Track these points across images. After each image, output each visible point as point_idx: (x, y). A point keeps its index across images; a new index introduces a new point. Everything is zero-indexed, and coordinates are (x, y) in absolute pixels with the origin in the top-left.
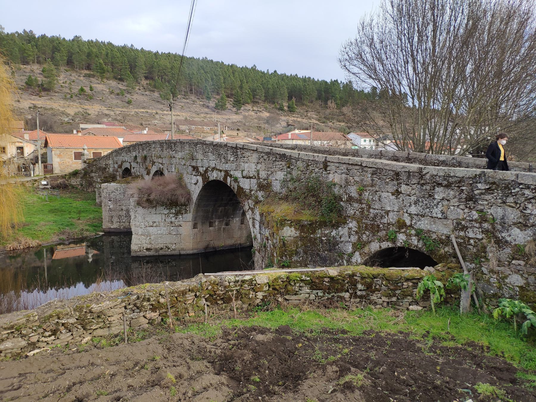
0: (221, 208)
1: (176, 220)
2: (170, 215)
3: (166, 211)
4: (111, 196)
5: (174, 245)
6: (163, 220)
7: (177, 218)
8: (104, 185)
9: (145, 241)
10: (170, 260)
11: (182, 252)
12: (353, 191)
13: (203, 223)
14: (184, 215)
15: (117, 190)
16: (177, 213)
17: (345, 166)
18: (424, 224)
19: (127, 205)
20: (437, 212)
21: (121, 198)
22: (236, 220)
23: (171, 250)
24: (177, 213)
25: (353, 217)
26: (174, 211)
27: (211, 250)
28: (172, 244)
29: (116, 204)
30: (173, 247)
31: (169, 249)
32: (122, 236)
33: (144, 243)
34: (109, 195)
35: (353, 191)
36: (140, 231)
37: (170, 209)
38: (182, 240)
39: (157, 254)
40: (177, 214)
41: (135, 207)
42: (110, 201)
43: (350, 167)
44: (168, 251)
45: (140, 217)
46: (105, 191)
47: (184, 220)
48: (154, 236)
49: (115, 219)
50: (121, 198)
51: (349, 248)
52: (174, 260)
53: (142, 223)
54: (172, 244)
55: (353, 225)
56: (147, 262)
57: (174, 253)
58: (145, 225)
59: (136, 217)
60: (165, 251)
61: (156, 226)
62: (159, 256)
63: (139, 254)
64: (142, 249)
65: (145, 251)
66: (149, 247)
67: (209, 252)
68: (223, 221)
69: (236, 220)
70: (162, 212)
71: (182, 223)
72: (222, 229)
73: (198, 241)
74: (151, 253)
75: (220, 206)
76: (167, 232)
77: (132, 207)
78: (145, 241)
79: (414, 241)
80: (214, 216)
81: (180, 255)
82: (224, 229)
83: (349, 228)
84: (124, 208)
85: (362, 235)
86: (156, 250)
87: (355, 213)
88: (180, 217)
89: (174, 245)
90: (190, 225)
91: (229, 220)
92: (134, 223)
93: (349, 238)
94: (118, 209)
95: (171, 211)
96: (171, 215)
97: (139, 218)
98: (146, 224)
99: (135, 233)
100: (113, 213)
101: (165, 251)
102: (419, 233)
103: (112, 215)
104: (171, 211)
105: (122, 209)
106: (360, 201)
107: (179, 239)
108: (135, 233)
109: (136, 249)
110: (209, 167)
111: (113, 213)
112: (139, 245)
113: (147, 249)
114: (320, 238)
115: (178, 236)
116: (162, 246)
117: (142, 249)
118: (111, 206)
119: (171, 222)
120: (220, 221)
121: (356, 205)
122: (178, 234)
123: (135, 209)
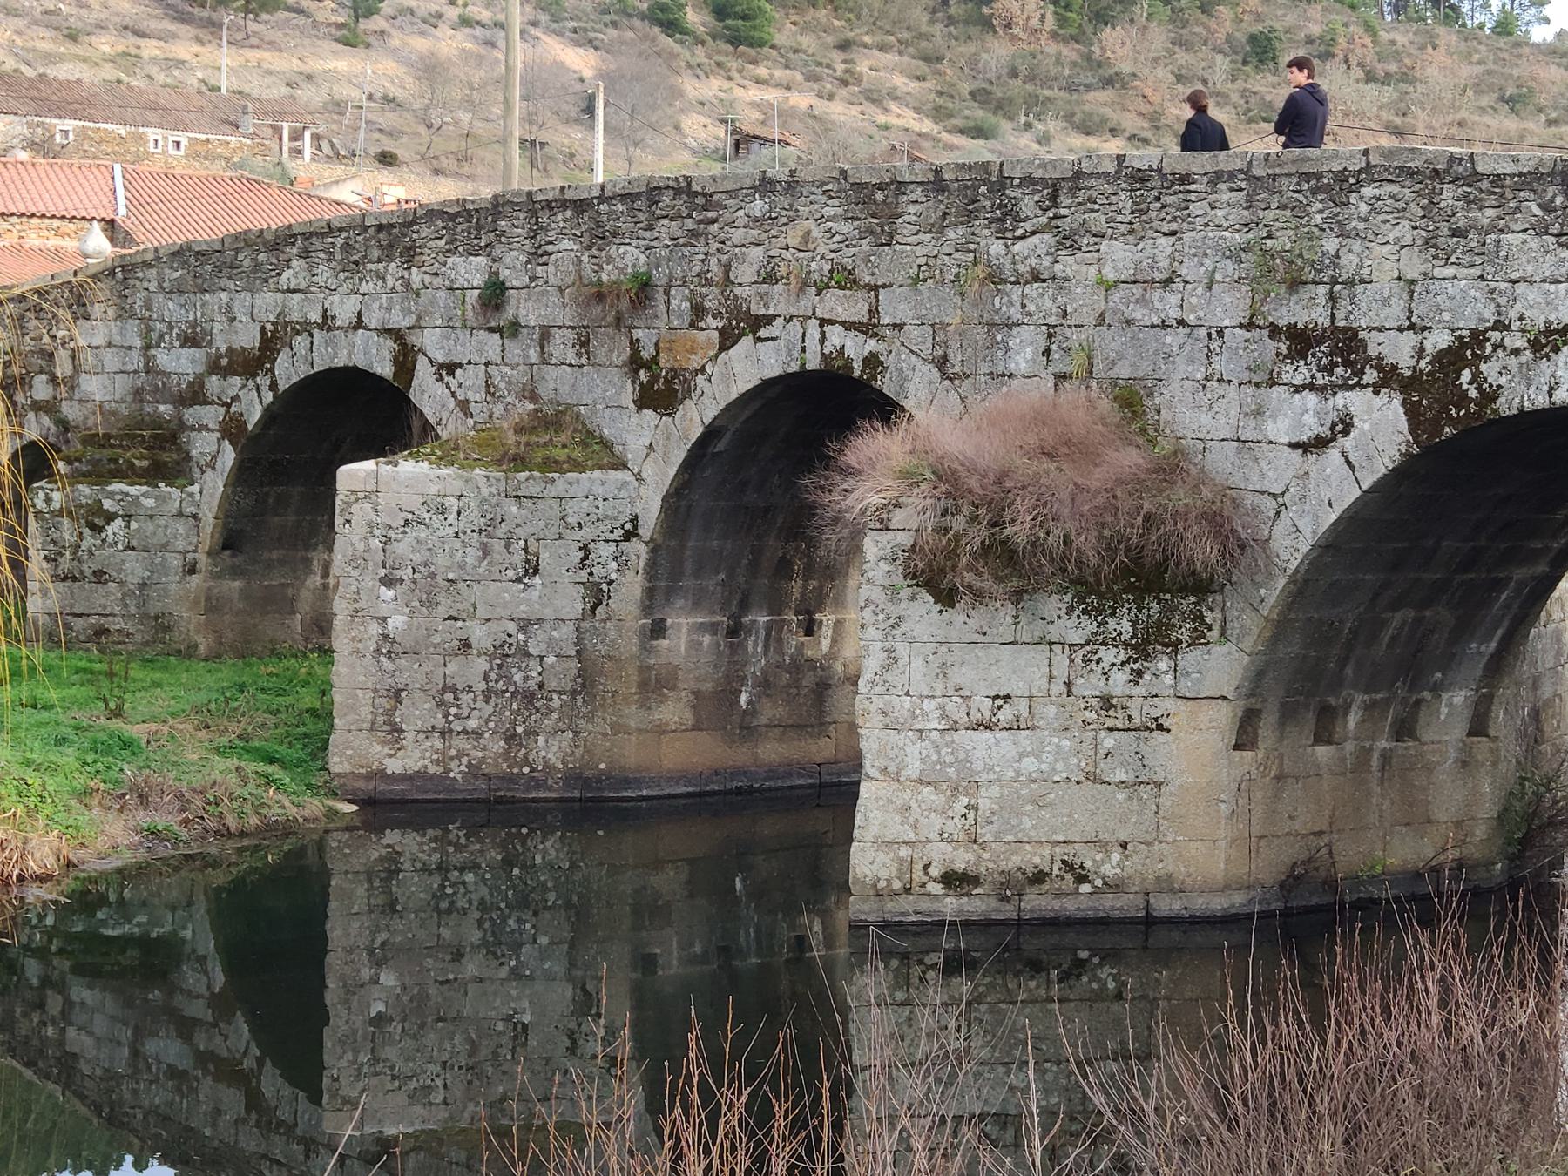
0: (1398, 617)
1: (1139, 690)
2: (1102, 650)
3: (1077, 629)
4: (402, 547)
5: (1116, 857)
6: (1058, 688)
7: (1140, 674)
8: (351, 474)
9: (937, 821)
10: (1084, 954)
11: (1166, 906)
13: (1288, 714)
14: (1190, 659)
15: (442, 510)
16: (1146, 642)
19: (499, 612)
21: (462, 566)
22: (1450, 705)
23: (1097, 891)
24: (1146, 642)
26: (1126, 627)
27: (1314, 901)
28: (1104, 846)
29: (430, 602)
30: (1109, 870)
31: (1083, 879)
32: (456, 832)
33: (934, 836)
34: (387, 541)
36: (914, 755)
37: (1100, 611)
38: (1164, 824)
39: (1008, 911)
40: (1142, 648)
41: (892, 591)
42: (388, 582)
44: (1076, 892)
45: (918, 663)
46: (362, 512)
47: (1186, 687)
48: (995, 791)
49: (418, 713)
50: (462, 566)
52: (1111, 956)
53: (928, 705)
54: (1104, 846)
56: (951, 967)
57: (1112, 904)
58: (944, 717)
59: (892, 658)
60: (1059, 894)
61: (1015, 726)
62: (1019, 924)
63: (905, 908)
64: (918, 875)
65: (936, 888)
66: (959, 866)
67: (1308, 910)
68: (1387, 702)
69: (1450, 705)
70: (1055, 632)
71: (1170, 705)
72: (1375, 762)
73: (1256, 831)
74: (977, 905)
75: (1394, 606)
76: (1073, 766)
77: (876, 594)
78: (937, 821)
80: (1349, 671)
81: (1150, 921)
82: (1386, 757)
84: (480, 635)
86: (1012, 885)
88: (1164, 664)
89: (1116, 857)
90: (1220, 719)
91: (1418, 702)
92: (878, 703)
94: (437, 639)
95: (1112, 623)
96: (1109, 655)
97: (916, 668)
98: (956, 709)
99: (884, 770)
100: (408, 672)
101: (1059, 894)
103: (401, 680)
104: (1112, 623)
105: (466, 645)
107: (1149, 814)
108: (884, 770)
109: (884, 874)
110: (1500, 326)
111: (408, 672)
112: (904, 852)
113: (955, 880)
115: (1145, 792)
116: (1037, 858)
117: (918, 875)
118: (397, 623)
119: (1107, 703)
120: (1369, 707)
122: (1145, 783)
123: (890, 608)
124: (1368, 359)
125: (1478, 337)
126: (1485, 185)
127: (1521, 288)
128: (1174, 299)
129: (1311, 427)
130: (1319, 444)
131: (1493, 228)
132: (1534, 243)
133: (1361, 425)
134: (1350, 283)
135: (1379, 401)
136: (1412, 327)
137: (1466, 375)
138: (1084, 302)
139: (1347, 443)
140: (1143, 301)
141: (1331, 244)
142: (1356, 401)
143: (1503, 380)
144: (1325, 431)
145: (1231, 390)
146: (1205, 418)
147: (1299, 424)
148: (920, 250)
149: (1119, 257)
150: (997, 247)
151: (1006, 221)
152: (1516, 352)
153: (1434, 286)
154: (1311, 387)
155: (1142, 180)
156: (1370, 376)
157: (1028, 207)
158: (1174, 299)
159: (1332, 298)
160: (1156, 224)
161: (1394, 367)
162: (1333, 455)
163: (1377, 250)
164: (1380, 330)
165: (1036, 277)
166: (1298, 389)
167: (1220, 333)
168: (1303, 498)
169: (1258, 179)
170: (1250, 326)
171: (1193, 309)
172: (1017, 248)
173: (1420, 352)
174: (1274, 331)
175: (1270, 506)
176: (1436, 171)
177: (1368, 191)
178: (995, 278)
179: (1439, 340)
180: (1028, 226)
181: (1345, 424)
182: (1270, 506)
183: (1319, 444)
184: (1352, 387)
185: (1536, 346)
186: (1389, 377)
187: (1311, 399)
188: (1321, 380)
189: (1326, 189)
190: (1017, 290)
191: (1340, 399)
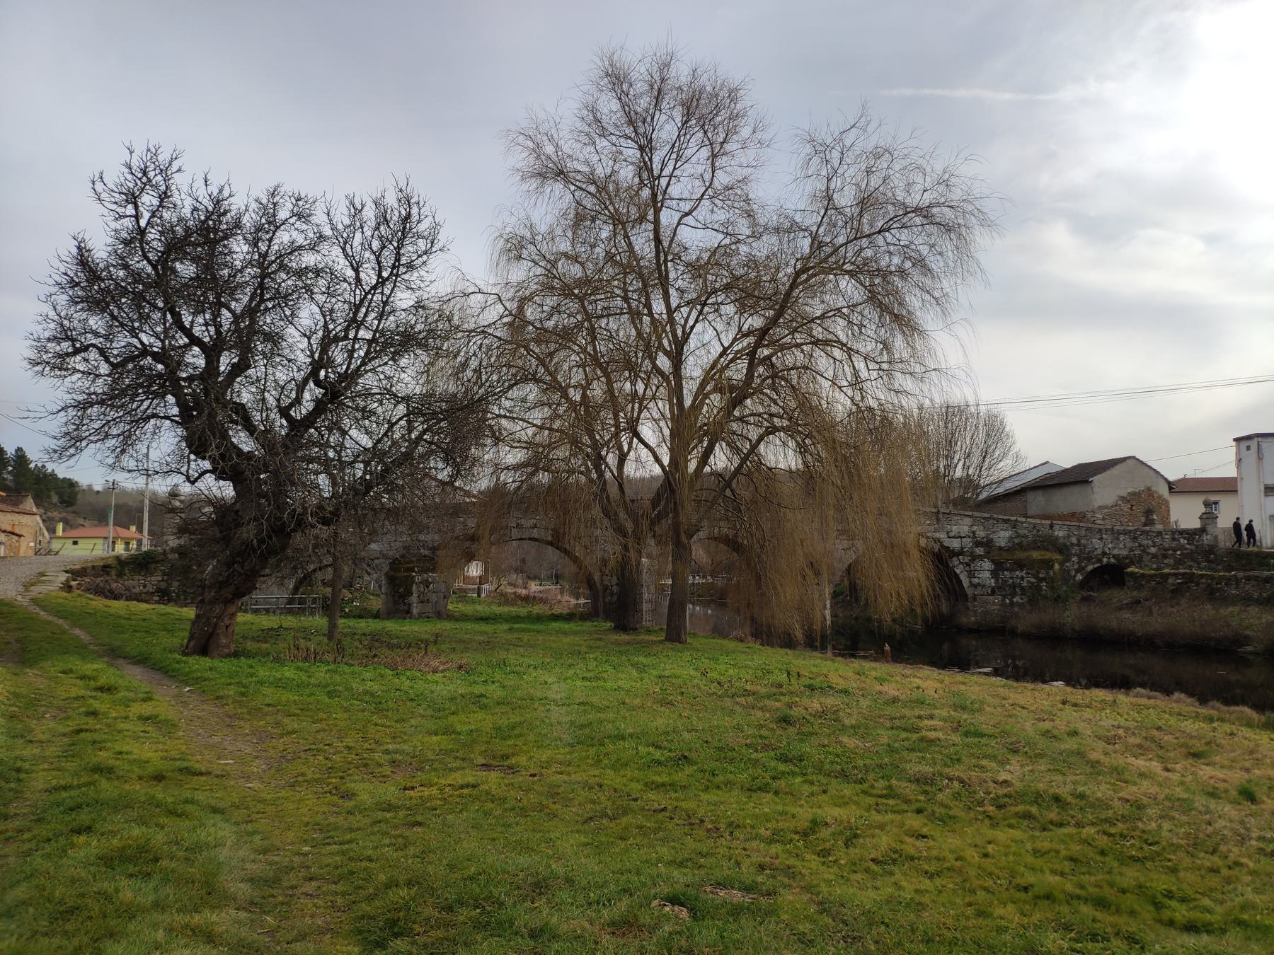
12: (1074, 540)
18: (1116, 552)
20: (1121, 546)
25: (1075, 555)
35: (1074, 540)
55: (1075, 559)
79: (1112, 560)
102: (1114, 556)
106: (1078, 545)
129: (845, 546)
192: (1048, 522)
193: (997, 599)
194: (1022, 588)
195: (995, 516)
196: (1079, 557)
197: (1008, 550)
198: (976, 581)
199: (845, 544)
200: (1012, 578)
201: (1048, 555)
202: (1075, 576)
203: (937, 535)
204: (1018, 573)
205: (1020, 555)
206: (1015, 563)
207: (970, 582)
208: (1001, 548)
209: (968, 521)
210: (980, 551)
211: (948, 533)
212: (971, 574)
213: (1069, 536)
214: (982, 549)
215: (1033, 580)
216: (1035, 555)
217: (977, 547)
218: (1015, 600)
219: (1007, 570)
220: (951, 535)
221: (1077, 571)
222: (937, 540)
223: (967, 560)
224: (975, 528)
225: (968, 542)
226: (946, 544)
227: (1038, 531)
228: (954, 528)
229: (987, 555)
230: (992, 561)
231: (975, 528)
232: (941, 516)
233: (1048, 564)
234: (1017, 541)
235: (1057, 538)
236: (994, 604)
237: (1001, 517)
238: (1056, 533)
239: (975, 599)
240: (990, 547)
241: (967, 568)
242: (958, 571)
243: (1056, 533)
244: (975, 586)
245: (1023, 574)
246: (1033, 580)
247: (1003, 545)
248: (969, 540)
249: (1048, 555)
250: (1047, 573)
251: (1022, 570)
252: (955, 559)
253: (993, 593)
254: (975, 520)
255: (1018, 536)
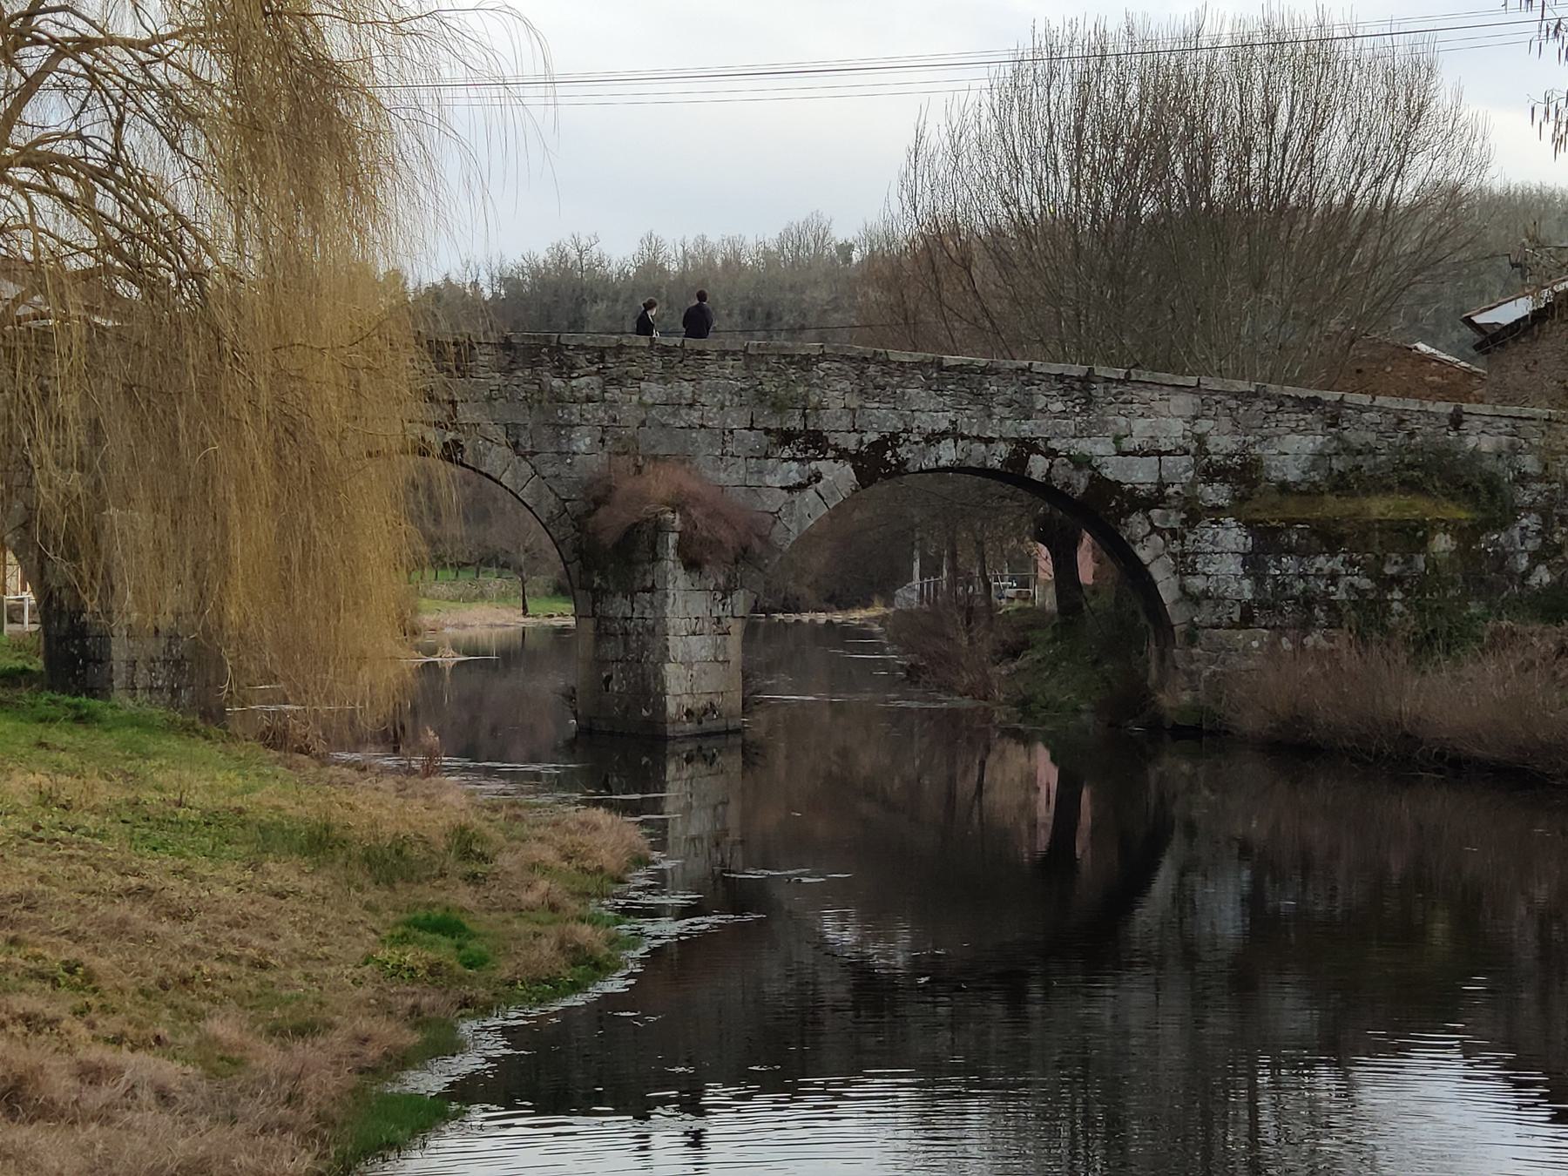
12: (1530, 464)
17: (1506, 421)
25: (1530, 509)
43: (1519, 423)
51: (1523, 562)
55: (1531, 521)
83: (1522, 529)
85: (1552, 534)
87: (1535, 499)
93: (1522, 544)
114: (1485, 549)
121: (1537, 486)
124: (829, 445)
125: (895, 436)
126: (893, 366)
127: (917, 414)
128: (697, 414)
129: (794, 478)
130: (801, 487)
131: (899, 385)
132: (924, 394)
133: (827, 477)
134: (816, 409)
135: (837, 466)
136: (855, 431)
137: (889, 453)
138: (629, 414)
139: (819, 486)
140: (674, 414)
141: (801, 390)
142: (822, 466)
143: (910, 456)
144: (805, 481)
145: (741, 461)
146: (723, 475)
147: (786, 477)
148: (492, 382)
149: (654, 391)
150: (556, 382)
151: (565, 369)
152: (917, 443)
153: (867, 412)
154: (794, 459)
155: (667, 352)
156: (831, 454)
157: (581, 361)
158: (697, 414)
159: (805, 416)
160: (681, 375)
161: (846, 450)
162: (810, 492)
163: (829, 393)
164: (836, 431)
165: (589, 399)
166: (785, 460)
167: (731, 432)
168: (791, 514)
169: (751, 355)
170: (751, 428)
171: (711, 419)
172: (574, 383)
173: (861, 442)
174: (768, 431)
175: (770, 519)
176: (866, 359)
177: (824, 365)
178: (558, 398)
179: (873, 437)
180: (581, 372)
181: (818, 477)
182: (770, 519)
183: (801, 487)
184: (820, 459)
185: (927, 440)
186: (842, 454)
187: (795, 465)
188: (799, 456)
189: (797, 363)
190: (576, 408)
191: (813, 465)
192: (1445, 408)
193: (1257, 639)
194: (1333, 607)
195: (1273, 388)
196: (1545, 517)
197: (1311, 492)
198: (1197, 583)
199: (793, 473)
200: (1303, 576)
201: (1418, 507)
202: (1527, 574)
203: (1084, 446)
204: (1321, 561)
205: (1332, 506)
206: (1314, 532)
207: (1182, 588)
208: (1284, 487)
209: (1184, 403)
210: (1216, 494)
211: (1117, 439)
212: (1184, 565)
213: (1514, 450)
214: (1225, 490)
215: (1365, 583)
216: (1379, 507)
217: (1209, 481)
218: (1309, 641)
219: (1290, 551)
220: (1126, 445)
221: (1536, 558)
222: (1081, 462)
223: (1175, 520)
224: (1204, 425)
225: (1180, 469)
226: (1109, 473)
227: (1411, 435)
228: (1139, 425)
229: (1239, 508)
230: (1249, 525)
231: (1204, 425)
232: (1098, 389)
233: (1411, 535)
234: (1338, 464)
235: (1476, 454)
236: (1247, 652)
237: (1290, 390)
238: (1471, 442)
239: (1191, 638)
240: (1254, 484)
241: (1176, 547)
242: (1144, 555)
243: (1471, 442)
244: (1192, 599)
245: (1336, 563)
246: (1365, 583)
247: (1293, 475)
248: (1186, 461)
249: (1418, 507)
250: (1408, 561)
251: (1333, 554)
252: (1136, 518)
253: (1247, 620)
254: (1207, 403)
255: (1348, 449)
